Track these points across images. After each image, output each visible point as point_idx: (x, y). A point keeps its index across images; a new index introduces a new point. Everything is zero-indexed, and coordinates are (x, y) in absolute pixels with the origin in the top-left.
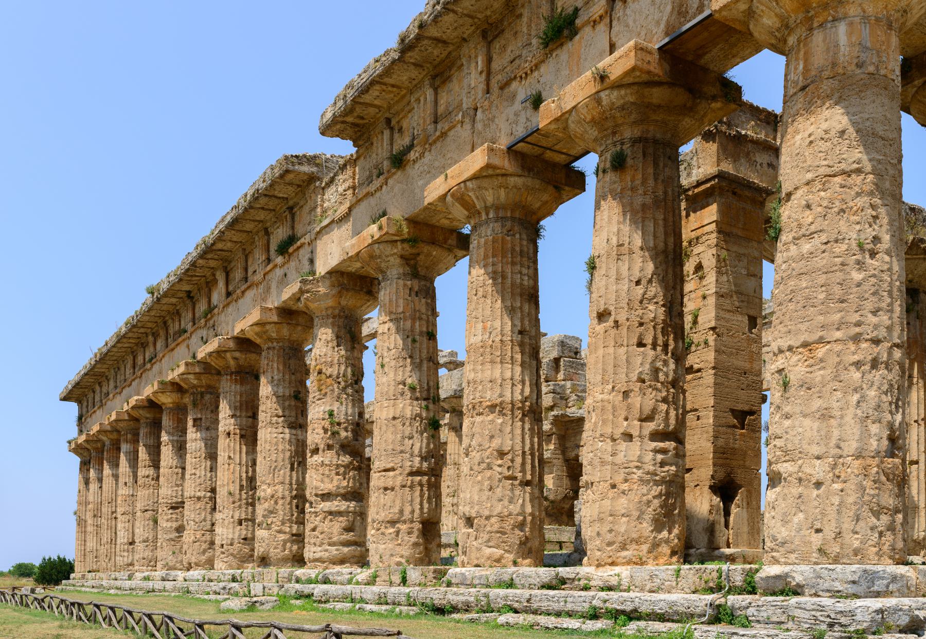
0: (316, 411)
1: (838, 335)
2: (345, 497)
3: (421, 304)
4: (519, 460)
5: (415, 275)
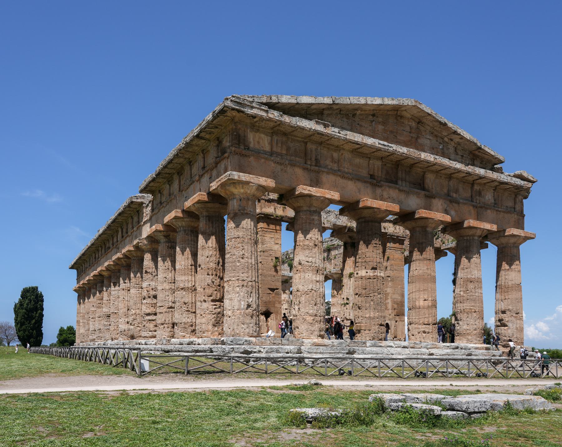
1: (234, 279)
4: (190, 305)
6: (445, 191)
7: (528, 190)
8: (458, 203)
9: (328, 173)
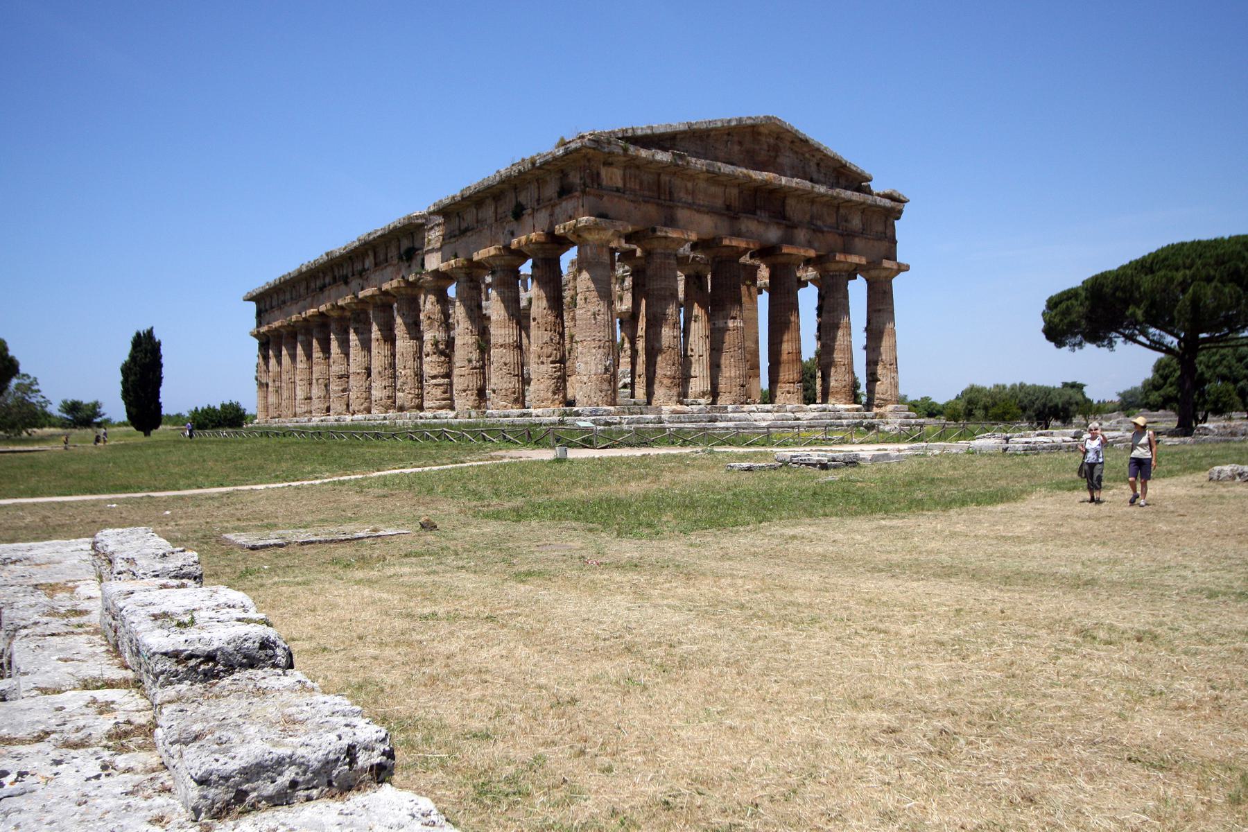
0: (428, 336)
2: (443, 377)
3: (475, 293)
5: (472, 281)
6: (808, 217)
7: (900, 212)
8: (822, 232)
9: (683, 208)
